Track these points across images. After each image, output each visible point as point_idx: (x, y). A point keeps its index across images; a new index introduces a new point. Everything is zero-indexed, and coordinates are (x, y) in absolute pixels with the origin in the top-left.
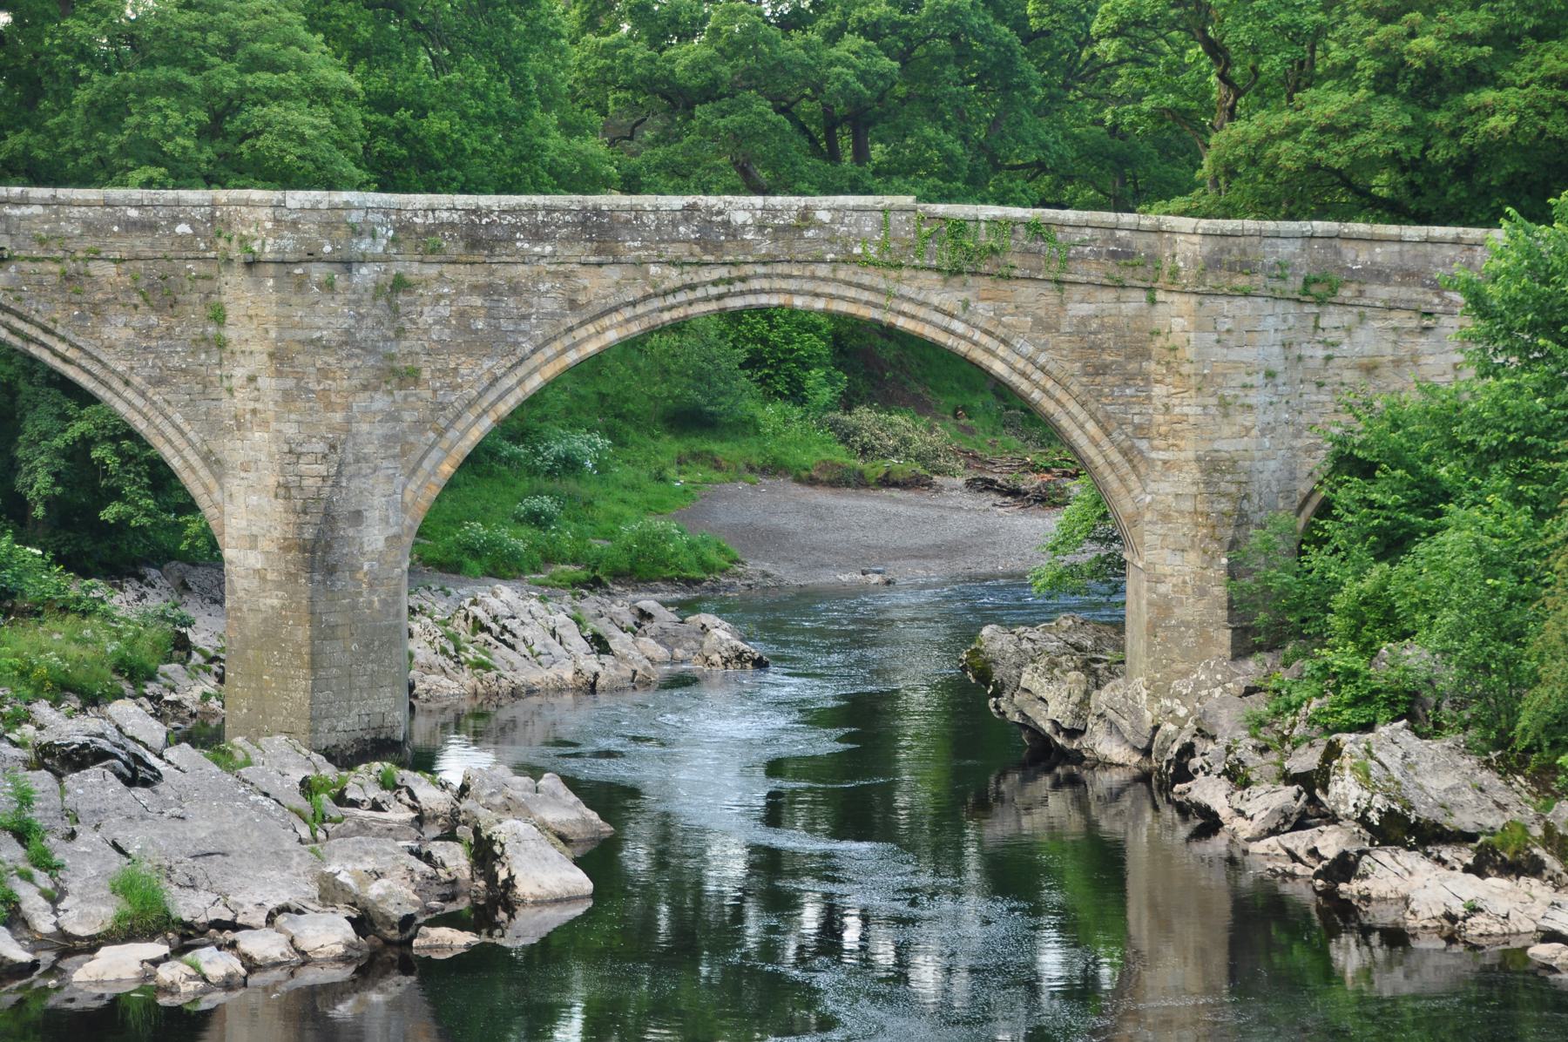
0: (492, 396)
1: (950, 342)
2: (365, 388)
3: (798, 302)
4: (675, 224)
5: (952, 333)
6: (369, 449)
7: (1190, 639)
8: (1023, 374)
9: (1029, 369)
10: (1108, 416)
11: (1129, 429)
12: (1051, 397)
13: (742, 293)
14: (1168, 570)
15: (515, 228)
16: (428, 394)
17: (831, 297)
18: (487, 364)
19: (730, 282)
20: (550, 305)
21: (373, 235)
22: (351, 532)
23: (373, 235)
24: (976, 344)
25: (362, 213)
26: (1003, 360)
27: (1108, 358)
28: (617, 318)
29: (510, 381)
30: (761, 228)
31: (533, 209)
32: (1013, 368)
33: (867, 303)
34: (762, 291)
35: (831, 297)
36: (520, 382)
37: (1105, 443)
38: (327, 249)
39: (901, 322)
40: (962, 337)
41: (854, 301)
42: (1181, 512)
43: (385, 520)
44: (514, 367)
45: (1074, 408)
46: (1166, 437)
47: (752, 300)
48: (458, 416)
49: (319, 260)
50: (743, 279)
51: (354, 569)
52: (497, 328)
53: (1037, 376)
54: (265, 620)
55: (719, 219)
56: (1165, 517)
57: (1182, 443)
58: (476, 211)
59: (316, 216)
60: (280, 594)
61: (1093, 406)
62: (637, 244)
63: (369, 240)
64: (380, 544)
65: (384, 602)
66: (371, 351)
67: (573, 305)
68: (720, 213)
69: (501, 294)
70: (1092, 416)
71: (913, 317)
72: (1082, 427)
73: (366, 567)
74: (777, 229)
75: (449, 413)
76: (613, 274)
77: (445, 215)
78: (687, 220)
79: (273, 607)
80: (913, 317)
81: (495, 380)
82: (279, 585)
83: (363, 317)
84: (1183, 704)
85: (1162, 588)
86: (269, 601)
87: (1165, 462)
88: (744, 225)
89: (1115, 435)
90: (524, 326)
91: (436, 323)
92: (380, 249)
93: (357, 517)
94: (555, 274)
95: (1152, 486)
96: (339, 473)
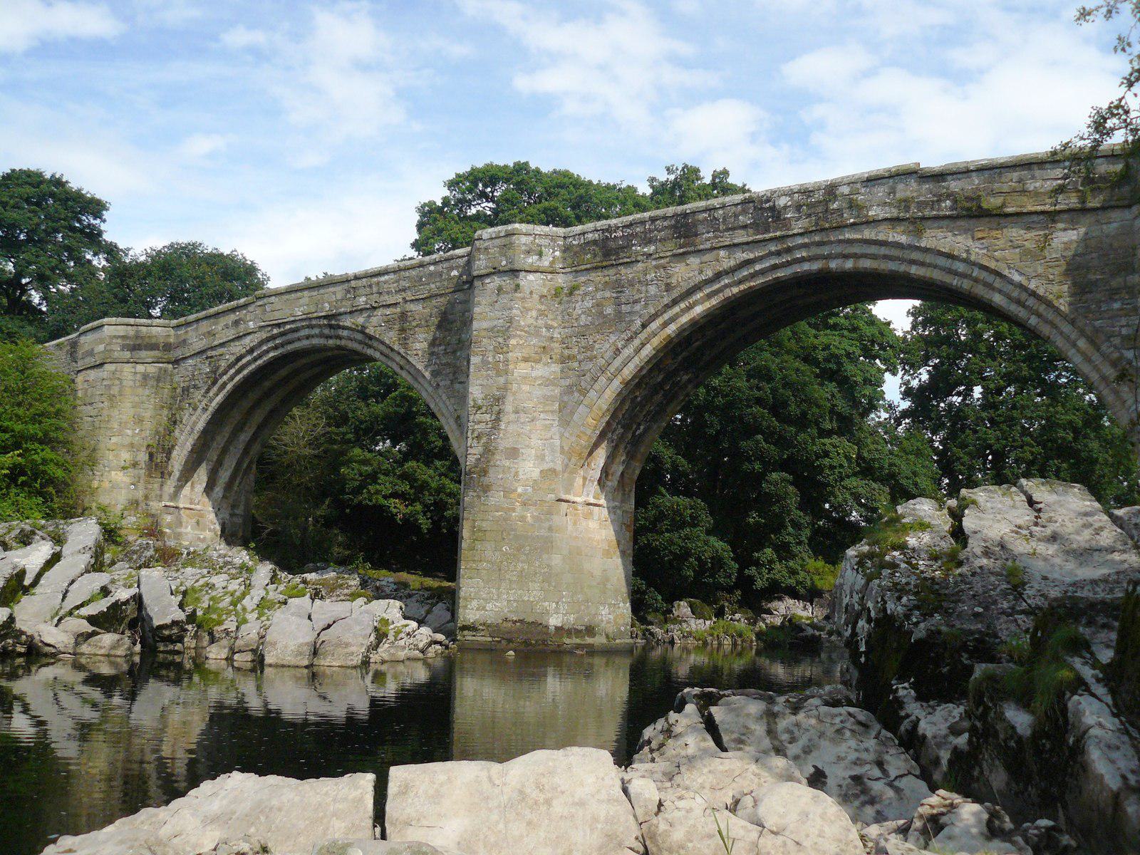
0: (617, 362)
1: (955, 282)
2: (526, 360)
3: (833, 265)
4: (736, 216)
5: (956, 273)
6: (529, 405)
9: (1024, 296)
10: (1097, 330)
11: (1117, 341)
12: (1047, 321)
13: (788, 264)
15: (632, 236)
16: (576, 365)
17: (856, 256)
18: (613, 338)
19: (778, 253)
20: (653, 290)
21: (540, 254)
22: (507, 463)
23: (540, 254)
24: (976, 280)
25: (531, 238)
26: (1000, 291)
27: (1092, 277)
28: (699, 295)
29: (627, 352)
30: (798, 208)
31: (643, 222)
32: (1009, 297)
33: (885, 257)
34: (803, 260)
35: (856, 256)
36: (638, 351)
37: (1096, 357)
38: (504, 263)
39: (914, 270)
40: (963, 276)
41: (874, 257)
43: (541, 458)
44: (630, 339)
45: (1066, 328)
47: (798, 269)
48: (595, 380)
49: (499, 272)
50: (789, 250)
51: (508, 492)
52: (620, 312)
53: (1031, 302)
55: (767, 205)
58: (609, 229)
59: (498, 242)
61: (1081, 322)
62: (711, 235)
63: (536, 257)
64: (536, 474)
65: (537, 519)
66: (537, 333)
67: (669, 288)
68: (768, 201)
69: (623, 287)
70: (1082, 333)
71: (922, 264)
72: (1074, 345)
73: (520, 490)
74: (810, 206)
75: (588, 377)
76: (694, 261)
77: (590, 236)
78: (744, 212)
80: (922, 264)
81: (617, 352)
83: (528, 310)
88: (785, 207)
89: (1104, 348)
90: (637, 307)
91: (583, 313)
92: (546, 264)
93: (513, 453)
94: (657, 267)
96: (498, 420)
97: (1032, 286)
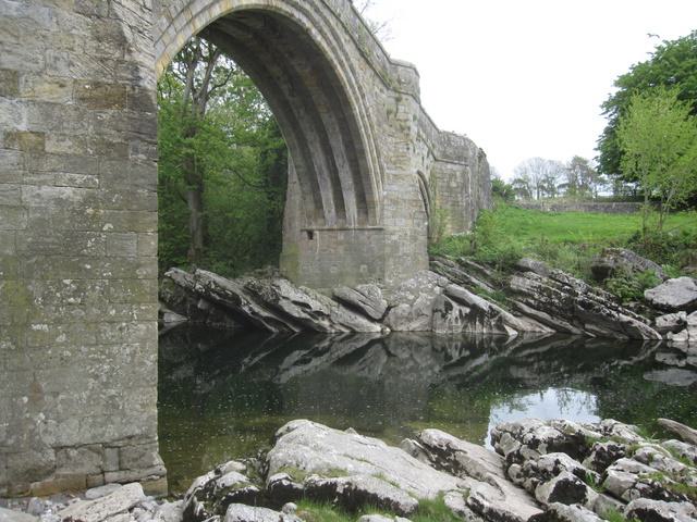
7: (409, 261)
8: (362, 117)
14: (397, 228)
42: (405, 201)
46: (395, 163)
53: (366, 119)
54: (41, 223)
56: (395, 202)
57: (404, 167)
60: (79, 178)
79: (59, 202)
82: (74, 163)
84: (412, 294)
85: (394, 238)
86: (46, 190)
87: (396, 175)
95: (387, 187)
97: (371, 110)
